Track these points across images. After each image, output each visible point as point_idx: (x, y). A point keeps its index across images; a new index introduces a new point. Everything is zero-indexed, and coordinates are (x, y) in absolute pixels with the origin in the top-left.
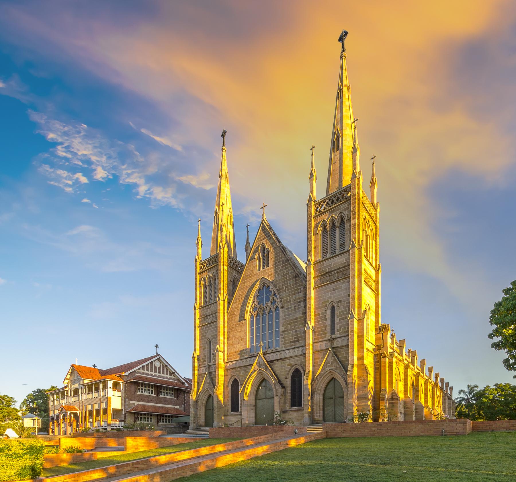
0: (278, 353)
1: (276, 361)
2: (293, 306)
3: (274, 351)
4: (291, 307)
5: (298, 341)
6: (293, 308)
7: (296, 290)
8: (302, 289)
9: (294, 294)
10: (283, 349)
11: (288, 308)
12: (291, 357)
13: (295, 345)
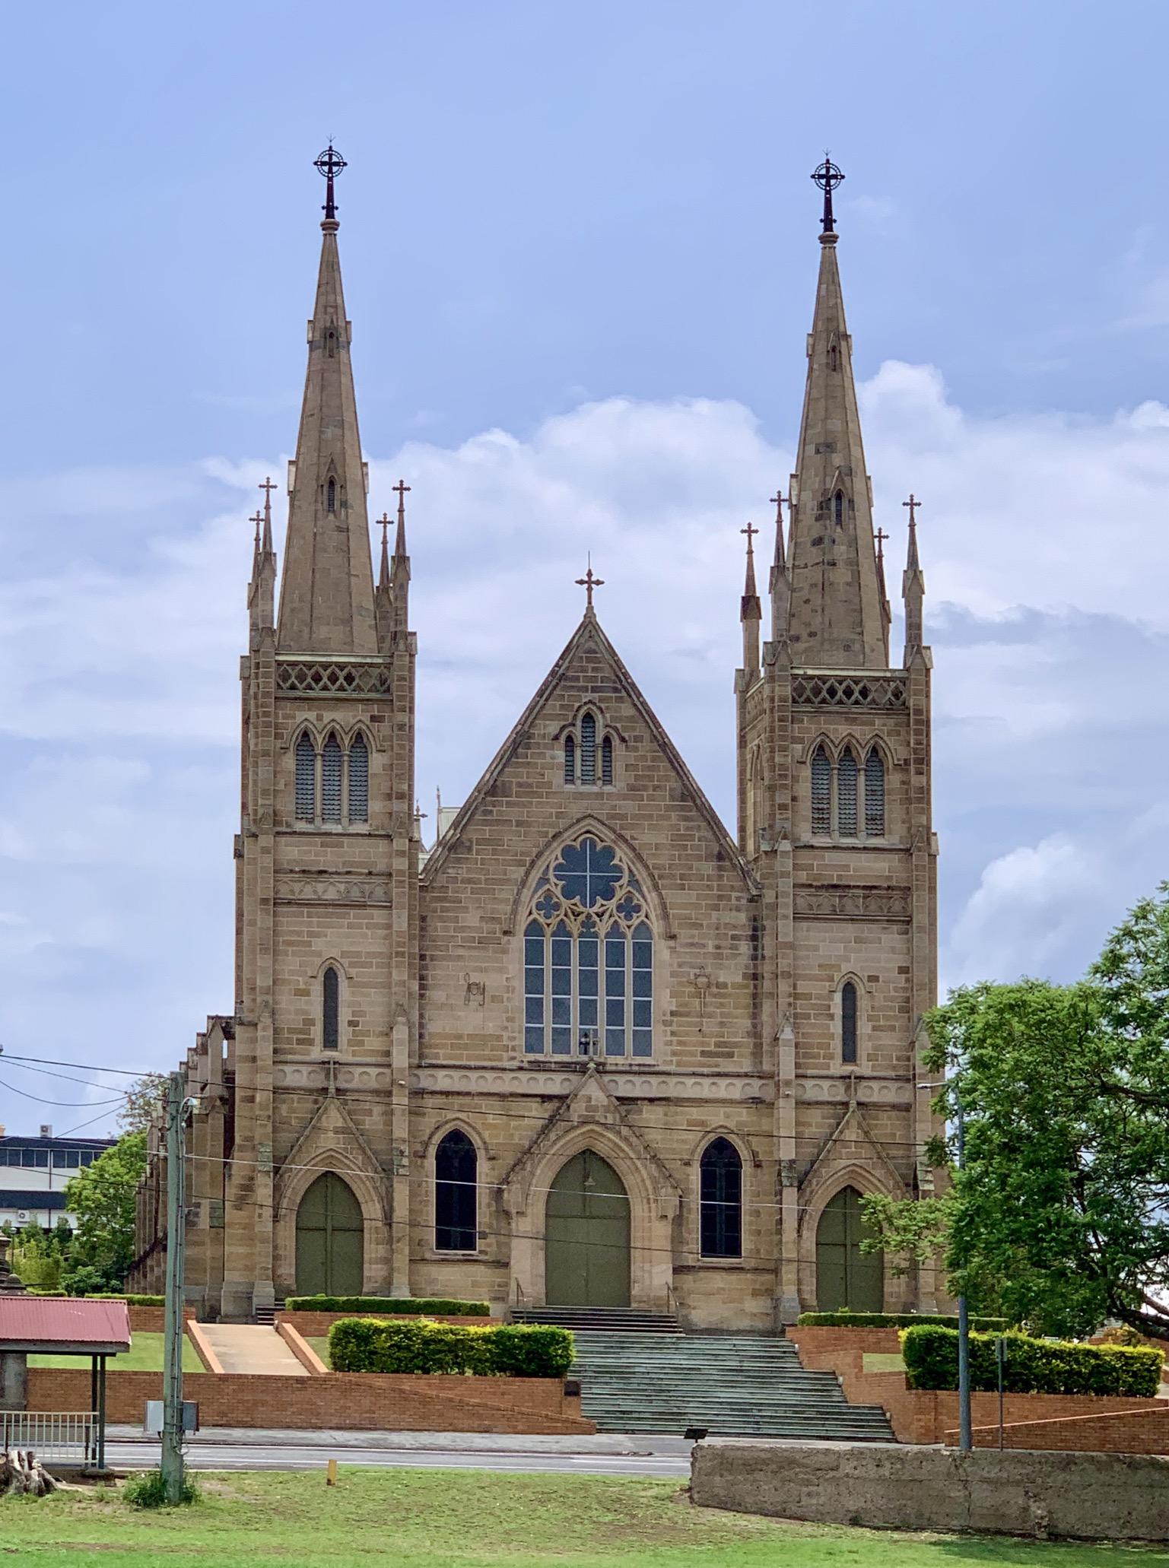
0: (654, 1080)
1: (646, 1102)
2: (711, 943)
3: (636, 1068)
4: (704, 946)
5: (731, 1055)
6: (711, 949)
7: (720, 897)
8: (744, 902)
9: (716, 908)
10: (672, 1068)
11: (692, 945)
12: (707, 1101)
13: (717, 1066)
